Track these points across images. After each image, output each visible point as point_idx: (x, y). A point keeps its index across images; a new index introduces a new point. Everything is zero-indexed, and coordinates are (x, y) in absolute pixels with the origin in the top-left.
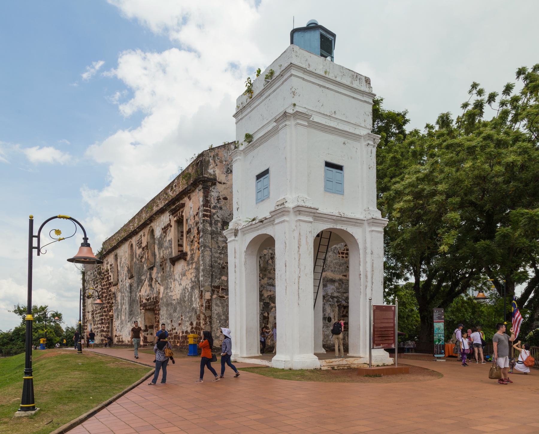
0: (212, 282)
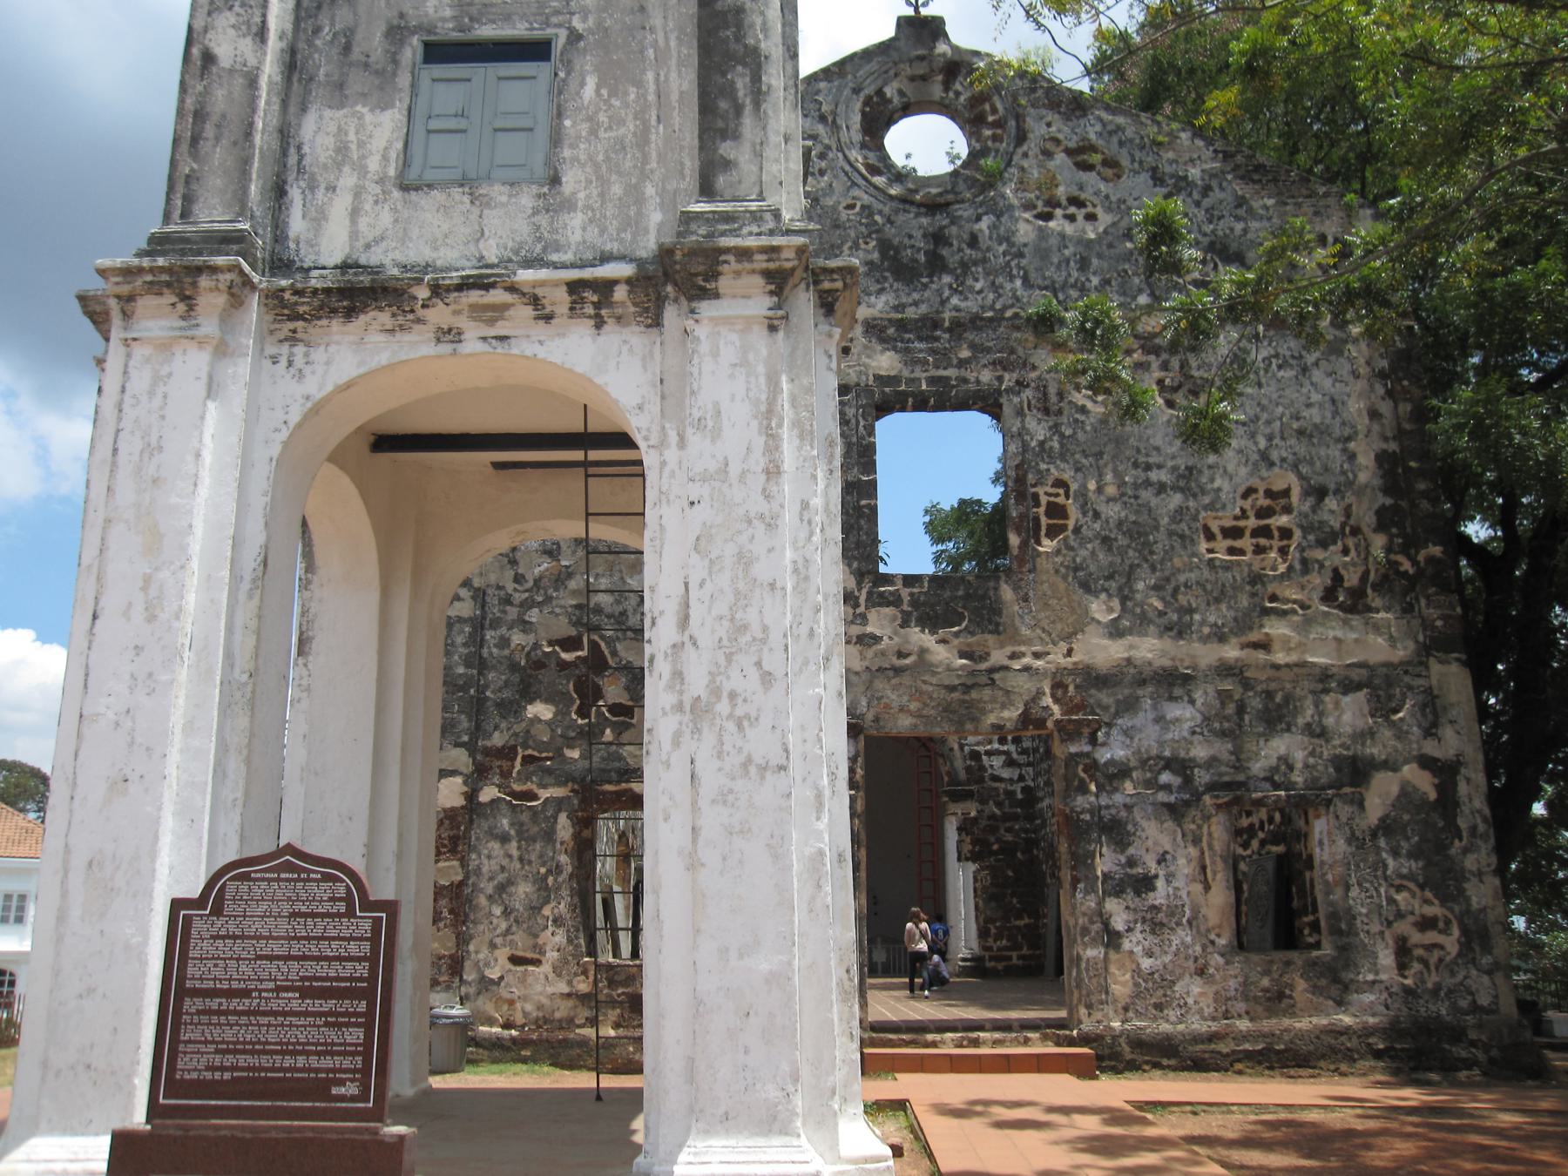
0: (478, 731)
